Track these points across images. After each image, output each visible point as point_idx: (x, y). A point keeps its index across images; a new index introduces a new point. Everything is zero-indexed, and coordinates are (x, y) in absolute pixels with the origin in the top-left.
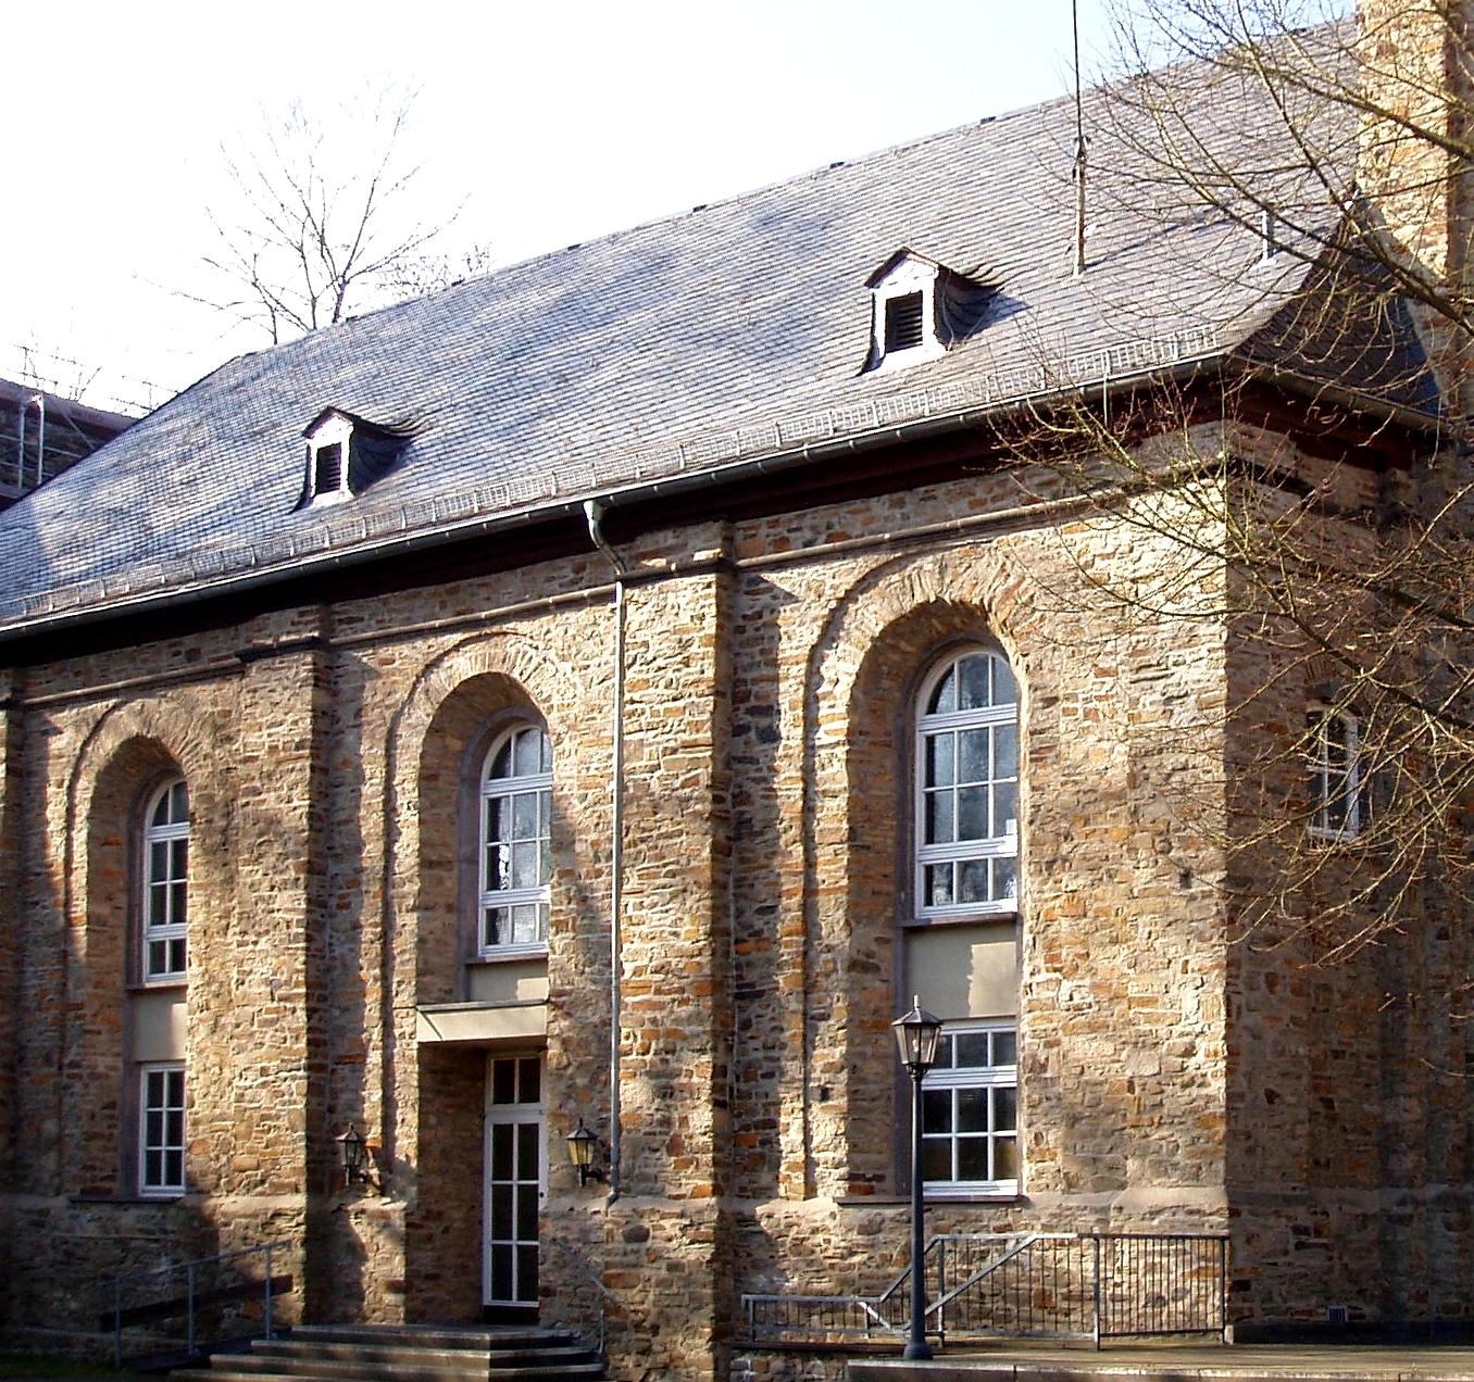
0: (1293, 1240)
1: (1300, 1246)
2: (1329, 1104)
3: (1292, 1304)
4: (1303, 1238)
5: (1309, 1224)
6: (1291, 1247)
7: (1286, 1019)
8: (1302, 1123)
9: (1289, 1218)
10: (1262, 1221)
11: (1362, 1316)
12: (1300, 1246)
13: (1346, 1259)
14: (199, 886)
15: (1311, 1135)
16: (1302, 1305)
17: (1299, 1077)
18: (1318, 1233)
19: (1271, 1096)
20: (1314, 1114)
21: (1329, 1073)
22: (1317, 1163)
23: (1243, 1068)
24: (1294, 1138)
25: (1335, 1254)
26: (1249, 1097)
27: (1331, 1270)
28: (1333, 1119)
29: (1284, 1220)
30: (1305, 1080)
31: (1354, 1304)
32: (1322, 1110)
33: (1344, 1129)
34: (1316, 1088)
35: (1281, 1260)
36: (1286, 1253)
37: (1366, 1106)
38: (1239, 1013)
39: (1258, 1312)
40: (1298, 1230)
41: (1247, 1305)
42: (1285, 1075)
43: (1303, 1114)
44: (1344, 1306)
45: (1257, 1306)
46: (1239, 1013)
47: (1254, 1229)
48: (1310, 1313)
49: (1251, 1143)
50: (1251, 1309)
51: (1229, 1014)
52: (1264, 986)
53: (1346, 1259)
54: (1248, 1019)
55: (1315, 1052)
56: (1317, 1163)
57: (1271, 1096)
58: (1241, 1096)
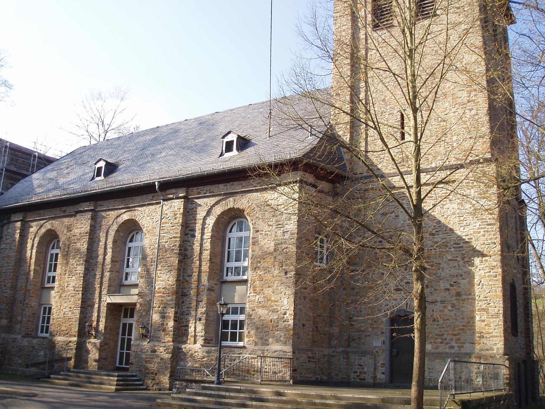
0: (307, 360)
1: (309, 361)
2: (317, 327)
3: (306, 375)
4: (310, 359)
5: (311, 356)
6: (307, 361)
7: (308, 307)
8: (310, 332)
9: (307, 354)
10: (300, 355)
11: (323, 379)
12: (309, 361)
13: (320, 365)
14: (60, 264)
15: (313, 335)
16: (309, 376)
17: (310, 321)
18: (313, 358)
19: (304, 325)
20: (313, 330)
21: (317, 320)
22: (314, 341)
23: (297, 318)
24: (309, 335)
25: (317, 364)
26: (298, 325)
27: (316, 367)
28: (318, 331)
30: (312, 322)
31: (321, 376)
32: (315, 329)
33: (320, 334)
34: (314, 324)
35: (304, 364)
37: (326, 329)
38: (297, 305)
39: (298, 377)
40: (309, 357)
41: (296, 375)
42: (307, 320)
43: (311, 329)
44: (319, 376)
45: (298, 375)
46: (297, 305)
47: (298, 357)
48: (311, 378)
49: (298, 336)
51: (294, 305)
52: (303, 299)
53: (320, 365)
54: (299, 307)
55: (314, 315)
56: (314, 341)
57: (304, 325)
58: (297, 325)
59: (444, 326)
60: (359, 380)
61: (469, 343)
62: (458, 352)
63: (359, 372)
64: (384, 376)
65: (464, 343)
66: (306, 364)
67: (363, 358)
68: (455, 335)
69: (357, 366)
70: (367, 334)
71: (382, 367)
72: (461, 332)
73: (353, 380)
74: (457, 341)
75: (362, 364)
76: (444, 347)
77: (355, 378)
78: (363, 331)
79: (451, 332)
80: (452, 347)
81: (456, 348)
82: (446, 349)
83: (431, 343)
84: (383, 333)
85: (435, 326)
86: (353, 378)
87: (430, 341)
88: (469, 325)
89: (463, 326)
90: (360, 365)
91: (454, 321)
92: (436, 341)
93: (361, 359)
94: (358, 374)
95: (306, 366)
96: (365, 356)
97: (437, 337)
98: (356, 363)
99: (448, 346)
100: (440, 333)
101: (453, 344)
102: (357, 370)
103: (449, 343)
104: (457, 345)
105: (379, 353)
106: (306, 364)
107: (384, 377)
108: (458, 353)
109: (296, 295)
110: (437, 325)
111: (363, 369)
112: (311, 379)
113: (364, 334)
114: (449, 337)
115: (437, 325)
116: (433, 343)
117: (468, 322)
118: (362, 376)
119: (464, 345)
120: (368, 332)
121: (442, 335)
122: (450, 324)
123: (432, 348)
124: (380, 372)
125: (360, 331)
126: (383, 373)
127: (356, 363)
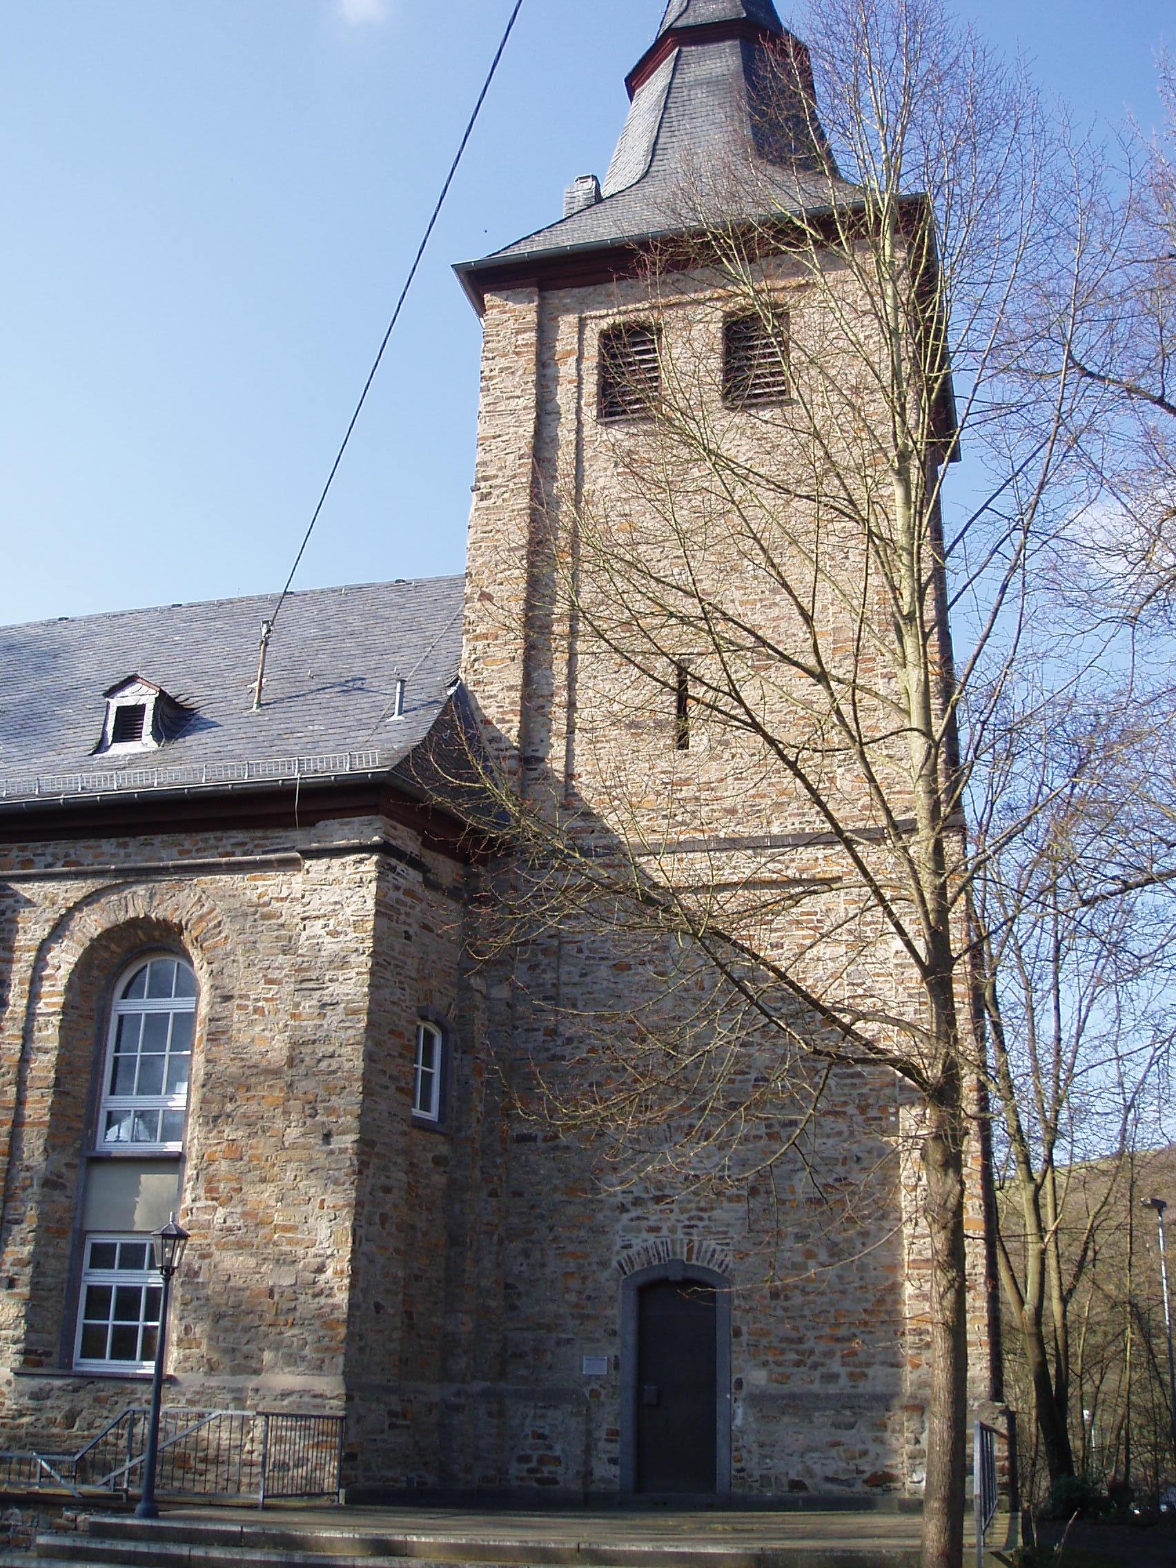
1: (392, 1426)
3: (384, 1473)
6: (386, 1427)
7: (391, 1250)
9: (385, 1404)
12: (392, 1426)
17: (397, 1294)
18: (404, 1416)
19: (378, 1307)
23: (361, 1285)
24: (391, 1340)
29: (382, 1406)
30: (400, 1297)
33: (419, 1335)
35: (378, 1437)
36: (382, 1431)
40: (391, 1414)
41: (353, 1473)
42: (387, 1291)
48: (396, 1480)
49: (362, 1343)
50: (356, 1477)
51: (354, 1243)
57: (378, 1307)
59: (806, 1312)
60: (535, 1485)
61: (883, 1363)
62: (848, 1391)
63: (535, 1459)
64: (615, 1470)
65: (869, 1365)
66: (384, 1436)
67: (550, 1412)
68: (838, 1340)
69: (530, 1441)
70: (564, 1336)
71: (611, 1441)
72: (857, 1332)
73: (516, 1483)
74: (847, 1360)
75: (547, 1432)
76: (805, 1377)
77: (522, 1479)
78: (549, 1328)
79: (827, 1331)
80: (832, 1378)
81: (843, 1381)
82: (812, 1382)
83: (765, 1364)
84: (614, 1333)
85: (780, 1313)
86: (518, 1478)
87: (763, 1358)
88: (883, 1308)
89: (865, 1311)
90: (542, 1437)
91: (837, 1296)
92: (780, 1358)
93: (543, 1416)
94: (534, 1464)
95: (383, 1441)
96: (556, 1407)
97: (784, 1345)
98: (528, 1430)
99: (817, 1374)
100: (794, 1335)
101: (836, 1367)
102: (529, 1452)
103: (823, 1365)
104: (848, 1369)
105: (602, 1398)
106: (384, 1436)
107: (618, 1473)
108: (849, 1396)
109: (360, 1210)
110: (785, 1309)
111: (550, 1448)
112: (397, 1485)
113: (554, 1335)
114: (822, 1347)
115: (785, 1309)
116: (772, 1366)
117: (879, 1301)
118: (546, 1471)
119: (867, 1371)
120: (564, 1331)
121: (800, 1340)
122: (823, 1308)
123: (770, 1380)
124: (605, 1457)
125: (540, 1326)
126: (613, 1461)
127: (528, 1430)
